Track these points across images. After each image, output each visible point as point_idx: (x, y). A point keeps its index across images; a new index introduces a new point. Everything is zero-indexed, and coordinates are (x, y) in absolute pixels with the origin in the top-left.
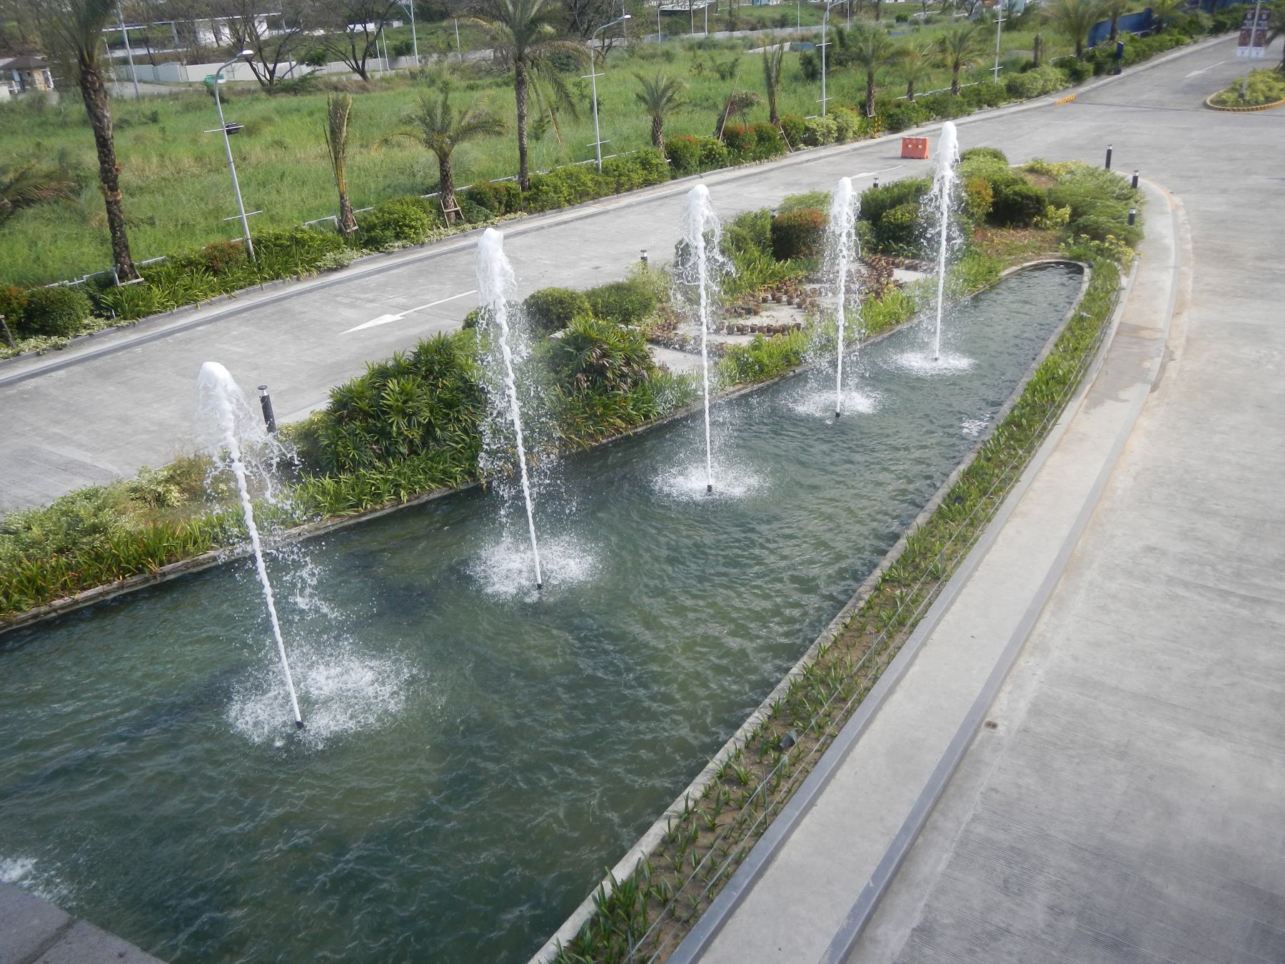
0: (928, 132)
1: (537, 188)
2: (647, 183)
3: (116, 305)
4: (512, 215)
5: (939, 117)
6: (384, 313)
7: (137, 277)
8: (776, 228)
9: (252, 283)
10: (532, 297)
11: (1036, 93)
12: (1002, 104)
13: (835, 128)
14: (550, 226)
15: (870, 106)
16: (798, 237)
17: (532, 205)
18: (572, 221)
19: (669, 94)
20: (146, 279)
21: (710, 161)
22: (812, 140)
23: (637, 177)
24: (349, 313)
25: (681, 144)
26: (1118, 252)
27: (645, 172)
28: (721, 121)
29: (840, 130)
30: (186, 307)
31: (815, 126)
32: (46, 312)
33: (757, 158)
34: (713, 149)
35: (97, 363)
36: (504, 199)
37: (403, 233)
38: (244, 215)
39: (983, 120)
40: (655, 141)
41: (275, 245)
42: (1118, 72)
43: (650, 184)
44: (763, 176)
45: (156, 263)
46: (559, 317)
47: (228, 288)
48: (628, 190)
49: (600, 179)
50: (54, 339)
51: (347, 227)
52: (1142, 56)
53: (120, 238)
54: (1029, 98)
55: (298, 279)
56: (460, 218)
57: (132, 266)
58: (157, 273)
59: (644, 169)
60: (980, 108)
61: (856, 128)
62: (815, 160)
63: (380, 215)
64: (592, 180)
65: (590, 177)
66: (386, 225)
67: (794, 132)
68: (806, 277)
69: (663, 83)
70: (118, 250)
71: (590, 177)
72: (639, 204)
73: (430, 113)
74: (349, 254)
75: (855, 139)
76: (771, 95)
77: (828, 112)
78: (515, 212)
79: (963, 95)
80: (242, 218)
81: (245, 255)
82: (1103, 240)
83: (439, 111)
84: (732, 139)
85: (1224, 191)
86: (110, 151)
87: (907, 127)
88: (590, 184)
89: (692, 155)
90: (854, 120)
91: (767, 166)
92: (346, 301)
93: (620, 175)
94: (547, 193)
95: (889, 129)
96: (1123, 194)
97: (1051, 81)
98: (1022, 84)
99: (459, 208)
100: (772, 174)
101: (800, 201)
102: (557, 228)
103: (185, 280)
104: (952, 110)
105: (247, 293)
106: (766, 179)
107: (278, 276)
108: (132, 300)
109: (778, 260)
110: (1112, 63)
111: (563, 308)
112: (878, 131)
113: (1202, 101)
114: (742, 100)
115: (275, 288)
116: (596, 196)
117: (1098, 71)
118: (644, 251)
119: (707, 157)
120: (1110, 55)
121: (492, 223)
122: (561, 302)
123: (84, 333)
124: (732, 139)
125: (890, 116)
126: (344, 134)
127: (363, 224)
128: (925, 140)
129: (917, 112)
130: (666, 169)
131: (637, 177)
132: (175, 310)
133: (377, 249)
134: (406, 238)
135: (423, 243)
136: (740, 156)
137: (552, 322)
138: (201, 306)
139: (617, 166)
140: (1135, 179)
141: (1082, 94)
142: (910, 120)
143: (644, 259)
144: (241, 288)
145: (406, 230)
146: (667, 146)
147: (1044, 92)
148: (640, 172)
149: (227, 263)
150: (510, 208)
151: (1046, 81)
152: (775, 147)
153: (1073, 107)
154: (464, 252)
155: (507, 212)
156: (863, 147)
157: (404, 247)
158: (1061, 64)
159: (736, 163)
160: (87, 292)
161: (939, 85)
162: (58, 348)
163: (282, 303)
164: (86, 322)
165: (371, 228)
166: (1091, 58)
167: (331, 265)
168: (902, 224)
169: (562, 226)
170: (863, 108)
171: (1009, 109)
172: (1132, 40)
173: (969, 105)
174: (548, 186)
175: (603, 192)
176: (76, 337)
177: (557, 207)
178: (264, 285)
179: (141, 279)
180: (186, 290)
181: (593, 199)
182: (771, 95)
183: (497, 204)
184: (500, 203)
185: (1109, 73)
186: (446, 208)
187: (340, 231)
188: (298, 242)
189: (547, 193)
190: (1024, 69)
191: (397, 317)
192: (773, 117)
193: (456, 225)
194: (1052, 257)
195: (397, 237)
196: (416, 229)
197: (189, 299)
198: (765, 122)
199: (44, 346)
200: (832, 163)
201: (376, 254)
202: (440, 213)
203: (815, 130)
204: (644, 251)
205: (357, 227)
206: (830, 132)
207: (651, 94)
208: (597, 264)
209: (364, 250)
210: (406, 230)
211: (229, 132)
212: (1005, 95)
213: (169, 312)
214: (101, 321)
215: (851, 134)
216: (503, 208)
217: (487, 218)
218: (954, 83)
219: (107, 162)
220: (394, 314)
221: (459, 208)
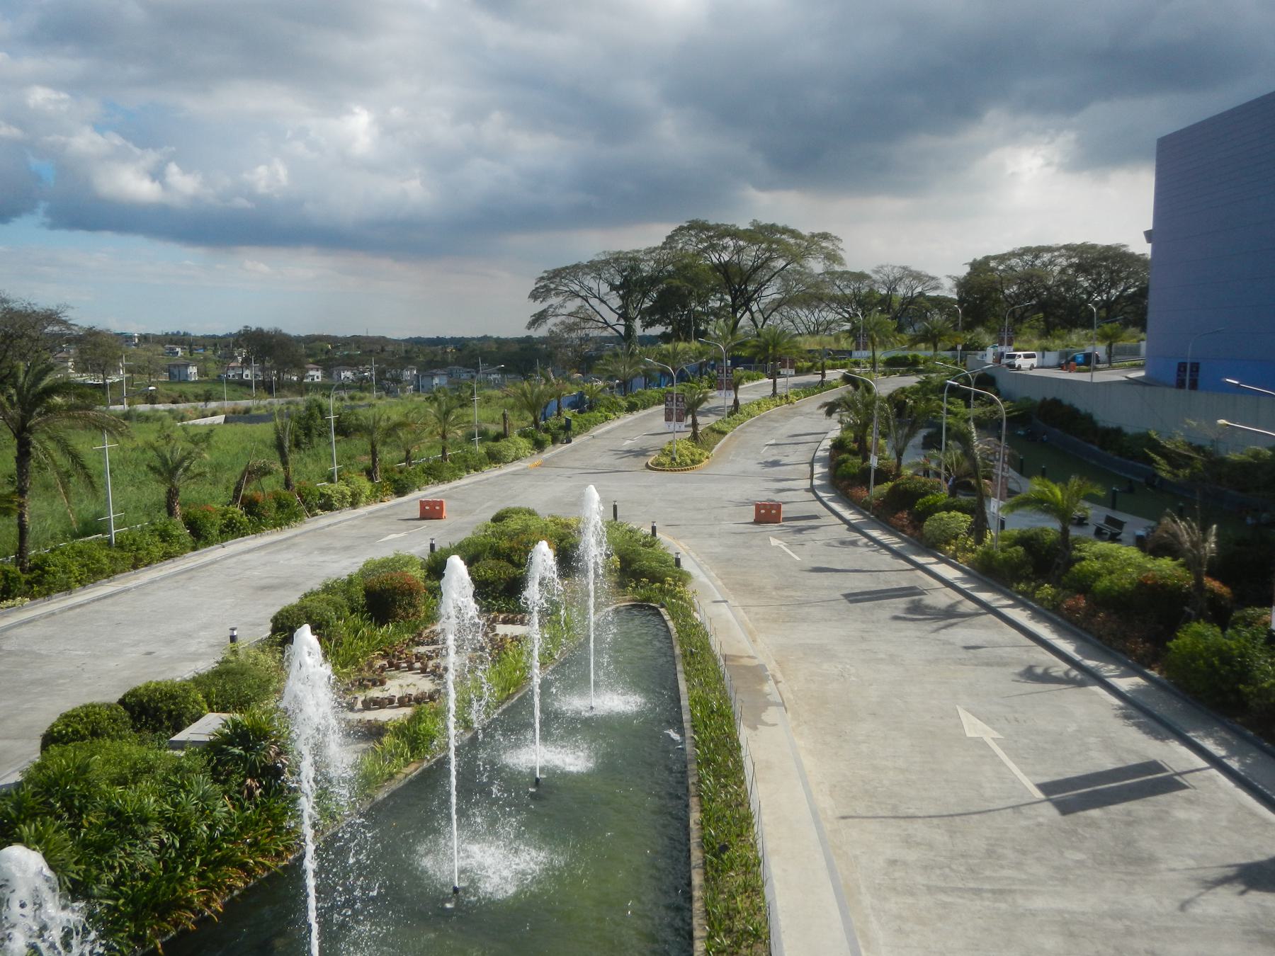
0: (431, 494)
1: (42, 569)
2: (168, 556)
4: (10, 602)
5: (437, 481)
8: (370, 594)
10: (133, 694)
12: (486, 469)
13: (349, 494)
14: (63, 611)
15: (375, 473)
16: (394, 601)
17: (36, 588)
18: (87, 604)
19: (186, 464)
21: (231, 530)
22: (328, 506)
23: (157, 551)
25: (199, 514)
26: (679, 592)
27: (165, 544)
28: (238, 490)
29: (354, 495)
31: (330, 492)
33: (278, 525)
34: (233, 518)
40: (171, 512)
42: (569, 441)
43: (171, 557)
44: (289, 542)
46: (169, 718)
48: (146, 566)
49: (116, 555)
52: (584, 428)
59: (164, 541)
60: (468, 472)
61: (368, 493)
62: (335, 524)
67: (310, 498)
68: (412, 640)
69: (177, 456)
72: (163, 579)
75: (368, 504)
77: (340, 478)
78: (14, 599)
79: (452, 461)
82: (663, 582)
84: (251, 506)
85: (711, 535)
87: (412, 491)
88: (105, 561)
89: (213, 524)
90: (366, 485)
91: (287, 533)
93: (138, 549)
94: (54, 575)
95: (396, 493)
97: (521, 449)
98: (499, 452)
100: (297, 540)
101: (384, 564)
102: (71, 613)
104: (447, 474)
109: (381, 626)
110: (564, 433)
111: (173, 704)
114: (259, 469)
116: (111, 574)
117: (555, 440)
118: (233, 629)
119: (227, 526)
120: (561, 428)
122: (173, 697)
124: (251, 506)
125: (395, 481)
128: (441, 503)
129: (420, 476)
136: (261, 523)
137: (161, 723)
139: (134, 540)
140: (654, 529)
141: (546, 460)
142: (414, 483)
143: (233, 639)
147: (517, 458)
151: (517, 449)
152: (295, 513)
153: (544, 471)
156: (377, 511)
158: (524, 434)
159: (257, 530)
161: (427, 451)
166: (547, 430)
168: (487, 580)
169: (78, 610)
170: (370, 473)
171: (492, 473)
172: (574, 416)
173: (460, 470)
174: (55, 566)
177: (67, 588)
181: (109, 576)
182: (285, 463)
189: (54, 575)
190: (498, 438)
192: (287, 484)
194: (625, 601)
198: (280, 489)
200: (354, 526)
203: (330, 497)
204: (233, 629)
208: (149, 649)
215: (364, 499)
218: (444, 452)
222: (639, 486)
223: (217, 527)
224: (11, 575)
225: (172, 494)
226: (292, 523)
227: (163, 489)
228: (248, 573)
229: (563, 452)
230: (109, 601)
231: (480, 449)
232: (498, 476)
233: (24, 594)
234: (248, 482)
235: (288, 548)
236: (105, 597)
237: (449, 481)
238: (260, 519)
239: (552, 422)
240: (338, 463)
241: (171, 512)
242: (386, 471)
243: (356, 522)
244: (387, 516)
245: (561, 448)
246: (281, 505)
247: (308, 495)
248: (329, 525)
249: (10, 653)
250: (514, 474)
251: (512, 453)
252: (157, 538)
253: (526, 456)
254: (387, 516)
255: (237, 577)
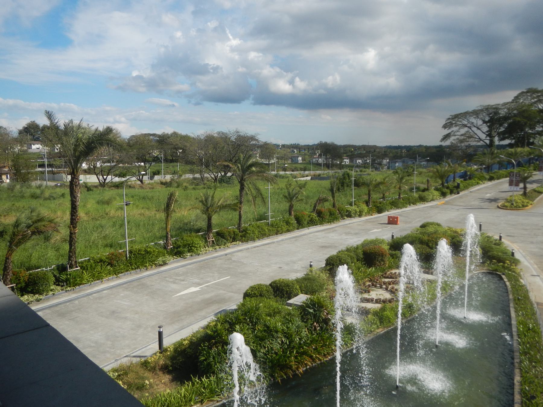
1: (246, 232)
2: (288, 231)
3: (67, 280)
4: (235, 243)
6: (192, 287)
7: (77, 267)
8: (365, 253)
9: (127, 271)
10: (274, 282)
11: (430, 200)
12: (418, 204)
14: (252, 248)
15: (370, 203)
16: (375, 258)
20: (81, 268)
21: (312, 223)
22: (349, 216)
23: (285, 229)
24: (174, 286)
25: (300, 215)
28: (315, 207)
29: (360, 212)
30: (98, 281)
31: (350, 210)
32: (36, 283)
33: (329, 222)
34: (313, 218)
35: (57, 309)
36: (232, 236)
37: (191, 249)
38: (127, 240)
39: (412, 210)
40: (290, 214)
41: (138, 254)
42: (458, 193)
45: (85, 261)
46: (287, 293)
47: (116, 273)
49: (270, 229)
50: (37, 296)
51: (168, 246)
52: (466, 187)
53: (73, 249)
54: (427, 202)
55: (146, 269)
56: (214, 243)
57: (76, 262)
58: (86, 265)
59: (287, 225)
60: (410, 205)
61: (366, 211)
62: (352, 223)
63: (182, 242)
64: (267, 229)
65: (267, 227)
66: (185, 246)
67: (342, 212)
68: (382, 275)
70: (71, 254)
71: (267, 227)
72: (286, 239)
73: (206, 200)
74: (168, 258)
75: (366, 216)
76: (333, 197)
79: (403, 200)
80: (126, 242)
81: (125, 258)
82: (504, 263)
83: (210, 199)
84: (320, 214)
85: (532, 243)
86: (77, 211)
87: (384, 211)
88: (267, 230)
89: (305, 220)
91: (333, 225)
92: (171, 280)
93: (278, 227)
96: (497, 243)
98: (425, 197)
99: (214, 239)
100: (336, 229)
101: (372, 242)
102: (255, 249)
103: (99, 268)
104: (400, 205)
105: (124, 275)
106: (335, 230)
107: (138, 267)
108: (75, 278)
109: (369, 268)
110: (456, 189)
111: (288, 288)
112: (374, 212)
113: (496, 206)
114: (324, 199)
115: (137, 273)
117: (451, 192)
118: (311, 262)
119: (310, 221)
120: (455, 187)
121: (227, 246)
122: (288, 286)
123: (51, 293)
124: (320, 214)
125: (378, 207)
126: (172, 207)
127: (174, 245)
128: (397, 218)
130: (296, 225)
131: (285, 228)
132: (92, 283)
133: (180, 256)
134: (192, 252)
135: (199, 254)
136: (323, 221)
137: (284, 295)
138: (104, 281)
139: (277, 224)
140: (500, 237)
142: (386, 208)
143: (311, 266)
144: (122, 273)
145: (193, 248)
146: (295, 216)
147: (433, 200)
148: (285, 226)
149: (117, 261)
150: (234, 240)
151: (433, 196)
153: (446, 206)
154: (218, 258)
155: (233, 241)
156: (369, 219)
157: (191, 256)
158: (437, 189)
159: (321, 223)
160: (53, 273)
161: (392, 195)
162: (38, 300)
163: (141, 280)
164: (52, 288)
165: (179, 247)
166: (448, 188)
167: (161, 263)
169: (257, 248)
170: (367, 203)
171: (421, 206)
172: (461, 182)
173: (406, 204)
175: (271, 234)
176: (46, 295)
177: (253, 240)
178: (132, 271)
179: (79, 268)
180: (99, 273)
181: (267, 237)
182: (333, 197)
183: (229, 238)
184: (231, 237)
185: (455, 194)
186: (209, 239)
187: (165, 248)
188: (147, 252)
190: (424, 190)
191: (197, 289)
192: (334, 206)
193: (212, 246)
194: (483, 270)
195: (189, 251)
196: (197, 248)
197: (98, 277)
198: (331, 207)
199: (31, 299)
200: (360, 225)
201: (179, 258)
202: (206, 241)
203: (351, 212)
204: (311, 262)
205: (172, 247)
206: (356, 212)
207: (289, 194)
209: (174, 257)
210: (193, 248)
211: (126, 205)
212: (419, 200)
213: (90, 284)
214: (59, 288)
215: (364, 214)
216: (231, 239)
217: (225, 244)
218: (399, 196)
219: (74, 216)
220: (196, 287)
221: (214, 239)
222: (493, 216)
223: (306, 221)
224: (236, 233)
225: (291, 207)
226: (335, 222)
227: (288, 205)
228: (317, 240)
229: (455, 198)
230: (267, 246)
231: (416, 195)
232: (423, 207)
233: (240, 240)
234: (319, 203)
235: (333, 232)
236: (266, 244)
237: (401, 208)
238: (323, 219)
239: (451, 184)
240: (354, 198)
241: (290, 214)
242: (374, 202)
243: (360, 223)
244: (374, 222)
245: (454, 196)
246: (331, 214)
247: (342, 211)
248: (349, 224)
249: (234, 261)
250: (431, 207)
251: (431, 197)
252: (285, 224)
253: (437, 199)
254: (374, 222)
255: (313, 241)
